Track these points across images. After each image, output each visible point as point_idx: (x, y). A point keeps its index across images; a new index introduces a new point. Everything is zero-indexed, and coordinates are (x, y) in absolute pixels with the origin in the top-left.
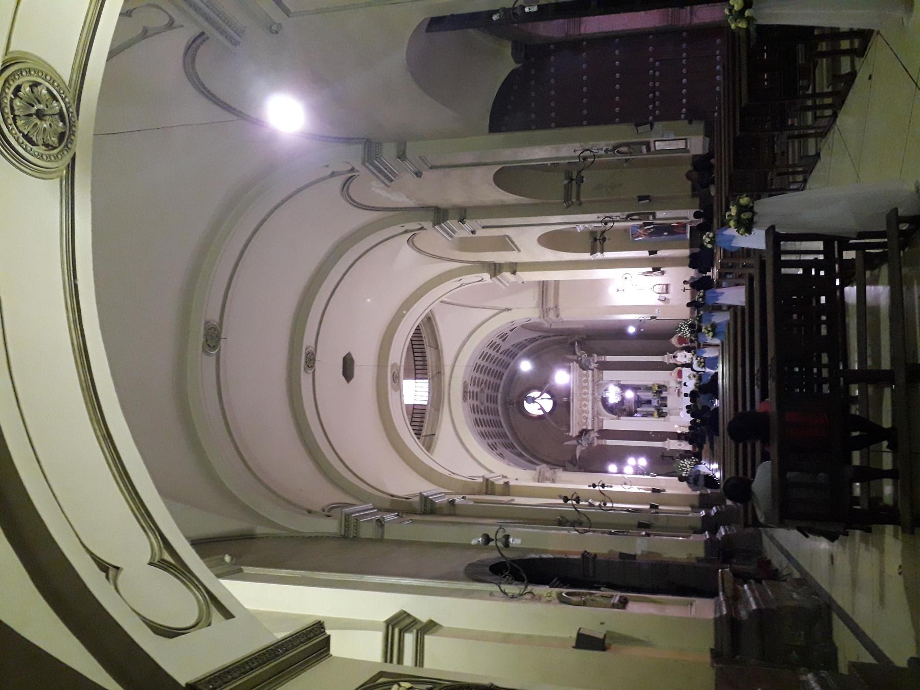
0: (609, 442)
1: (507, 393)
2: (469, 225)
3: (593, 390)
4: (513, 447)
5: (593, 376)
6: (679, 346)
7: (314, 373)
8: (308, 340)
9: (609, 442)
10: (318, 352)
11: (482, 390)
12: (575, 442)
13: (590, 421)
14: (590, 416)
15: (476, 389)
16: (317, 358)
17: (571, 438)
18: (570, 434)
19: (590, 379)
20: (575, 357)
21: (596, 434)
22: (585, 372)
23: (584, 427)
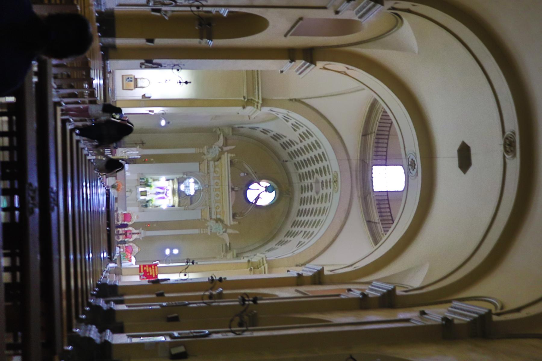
0: (192, 151)
1: (291, 199)
2: (356, 294)
3: (210, 199)
4: (285, 146)
5: (210, 213)
6: (131, 244)
7: (504, 132)
8: (514, 164)
9: (192, 151)
10: (502, 157)
11: (317, 193)
12: (225, 149)
13: (212, 170)
14: (212, 175)
15: (324, 192)
16: (502, 148)
17: (229, 152)
18: (229, 155)
19: (213, 210)
20: (230, 231)
21: (205, 157)
22: (218, 216)
23: (216, 163)
